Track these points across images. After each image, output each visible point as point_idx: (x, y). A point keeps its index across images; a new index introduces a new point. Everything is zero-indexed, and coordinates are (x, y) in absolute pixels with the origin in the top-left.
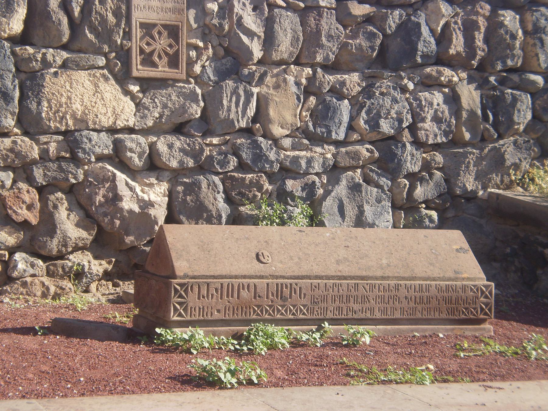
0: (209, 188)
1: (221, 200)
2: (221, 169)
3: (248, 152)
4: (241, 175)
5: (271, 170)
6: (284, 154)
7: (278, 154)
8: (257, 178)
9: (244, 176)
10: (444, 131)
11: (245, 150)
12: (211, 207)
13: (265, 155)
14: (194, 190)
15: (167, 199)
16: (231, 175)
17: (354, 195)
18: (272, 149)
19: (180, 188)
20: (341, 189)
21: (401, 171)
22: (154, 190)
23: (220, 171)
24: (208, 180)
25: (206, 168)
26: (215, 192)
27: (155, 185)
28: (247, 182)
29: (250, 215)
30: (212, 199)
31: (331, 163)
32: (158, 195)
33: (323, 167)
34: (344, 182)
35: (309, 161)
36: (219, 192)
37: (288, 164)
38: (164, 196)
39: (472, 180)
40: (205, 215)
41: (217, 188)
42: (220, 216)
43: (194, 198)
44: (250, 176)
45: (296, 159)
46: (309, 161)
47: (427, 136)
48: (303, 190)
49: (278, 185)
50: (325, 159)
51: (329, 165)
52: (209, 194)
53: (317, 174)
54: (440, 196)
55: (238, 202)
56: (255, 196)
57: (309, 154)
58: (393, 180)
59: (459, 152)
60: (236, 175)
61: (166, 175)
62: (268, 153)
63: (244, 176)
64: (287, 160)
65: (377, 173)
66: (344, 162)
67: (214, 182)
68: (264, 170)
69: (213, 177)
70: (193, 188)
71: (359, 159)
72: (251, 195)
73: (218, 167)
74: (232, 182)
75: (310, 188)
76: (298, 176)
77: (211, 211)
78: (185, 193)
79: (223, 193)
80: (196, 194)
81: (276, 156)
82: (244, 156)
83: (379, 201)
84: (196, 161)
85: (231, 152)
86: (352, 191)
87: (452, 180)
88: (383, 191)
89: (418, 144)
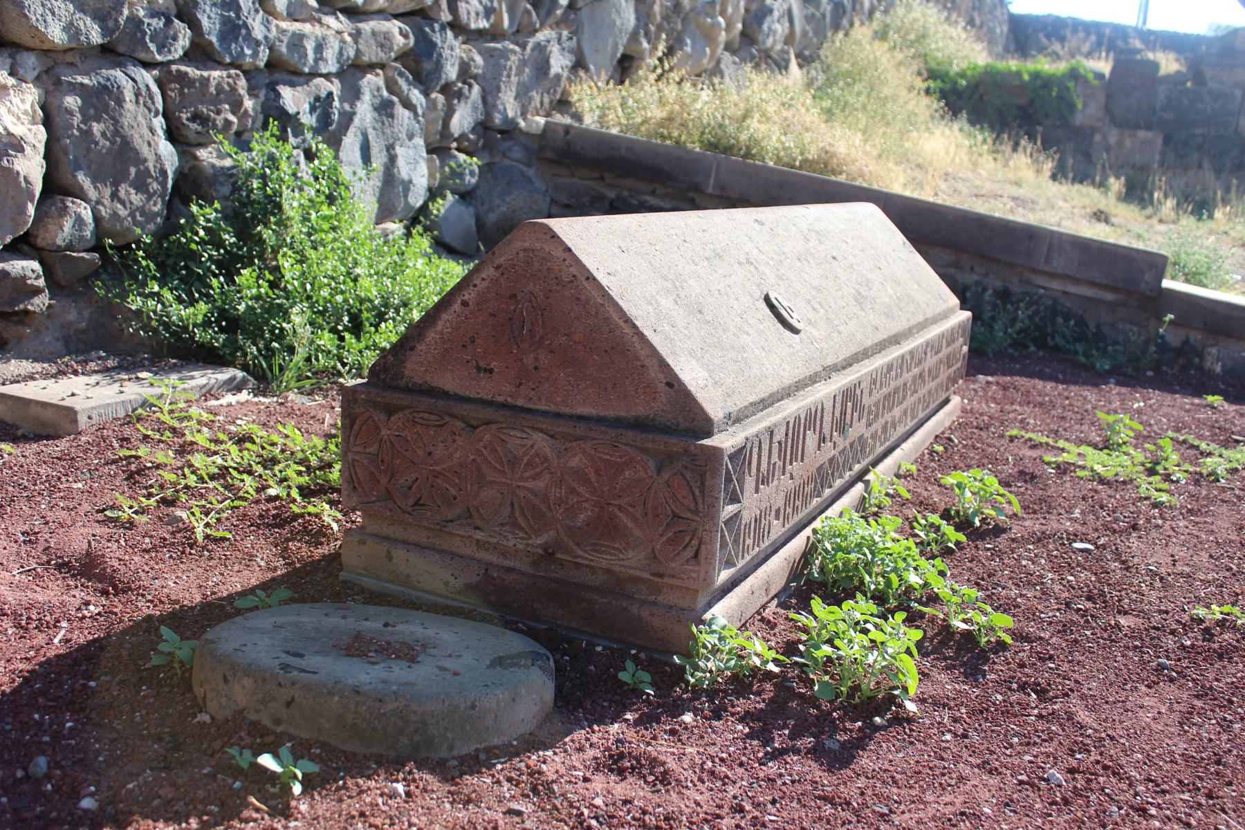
0: (137, 102)
1: (160, 132)
2: (159, 53)
3: (213, 16)
4: (198, 72)
5: (253, 63)
6: (277, 26)
7: (266, 24)
8: (231, 81)
9: (205, 74)
10: (485, 7)
11: (208, 9)
12: (145, 151)
13: (245, 25)
14: (107, 105)
15: (42, 128)
16: (178, 71)
17: (383, 123)
18: (257, 11)
19: (72, 102)
20: (364, 111)
21: (440, 78)
22: (8, 103)
23: (159, 58)
24: (133, 80)
25: (121, 49)
26: (150, 110)
27: (12, 92)
28: (212, 90)
29: (222, 168)
30: (145, 131)
31: (352, 53)
32: (19, 118)
33: (338, 62)
34: (367, 97)
35: (319, 48)
36: (156, 114)
37: (284, 50)
38: (34, 123)
39: (512, 100)
40: (133, 170)
41: (153, 103)
42: (163, 173)
43: (108, 128)
44: (216, 74)
45: (297, 41)
46: (319, 48)
47: (469, 13)
48: (313, 109)
49: (262, 98)
50: (343, 41)
51: (348, 58)
52: (140, 118)
53: (327, 76)
54: (473, 130)
55: (192, 137)
56: (228, 123)
57: (318, 31)
58: (426, 94)
59: (496, 49)
60: (189, 70)
61: (30, 63)
62: (250, 21)
63: (205, 74)
64: (282, 41)
65: (407, 79)
66: (371, 53)
67: (147, 86)
68: (240, 62)
69: (143, 71)
70: (102, 101)
71: (391, 49)
72: (220, 121)
73: (153, 47)
74: (181, 90)
75: (322, 105)
76: (295, 79)
77: (145, 160)
78: (86, 119)
79: (164, 116)
80: (113, 118)
81: (263, 28)
82: (205, 23)
83: (411, 137)
84: (105, 31)
85: (174, 11)
86: (380, 114)
87: (489, 98)
88: (416, 114)
89: (457, 27)
